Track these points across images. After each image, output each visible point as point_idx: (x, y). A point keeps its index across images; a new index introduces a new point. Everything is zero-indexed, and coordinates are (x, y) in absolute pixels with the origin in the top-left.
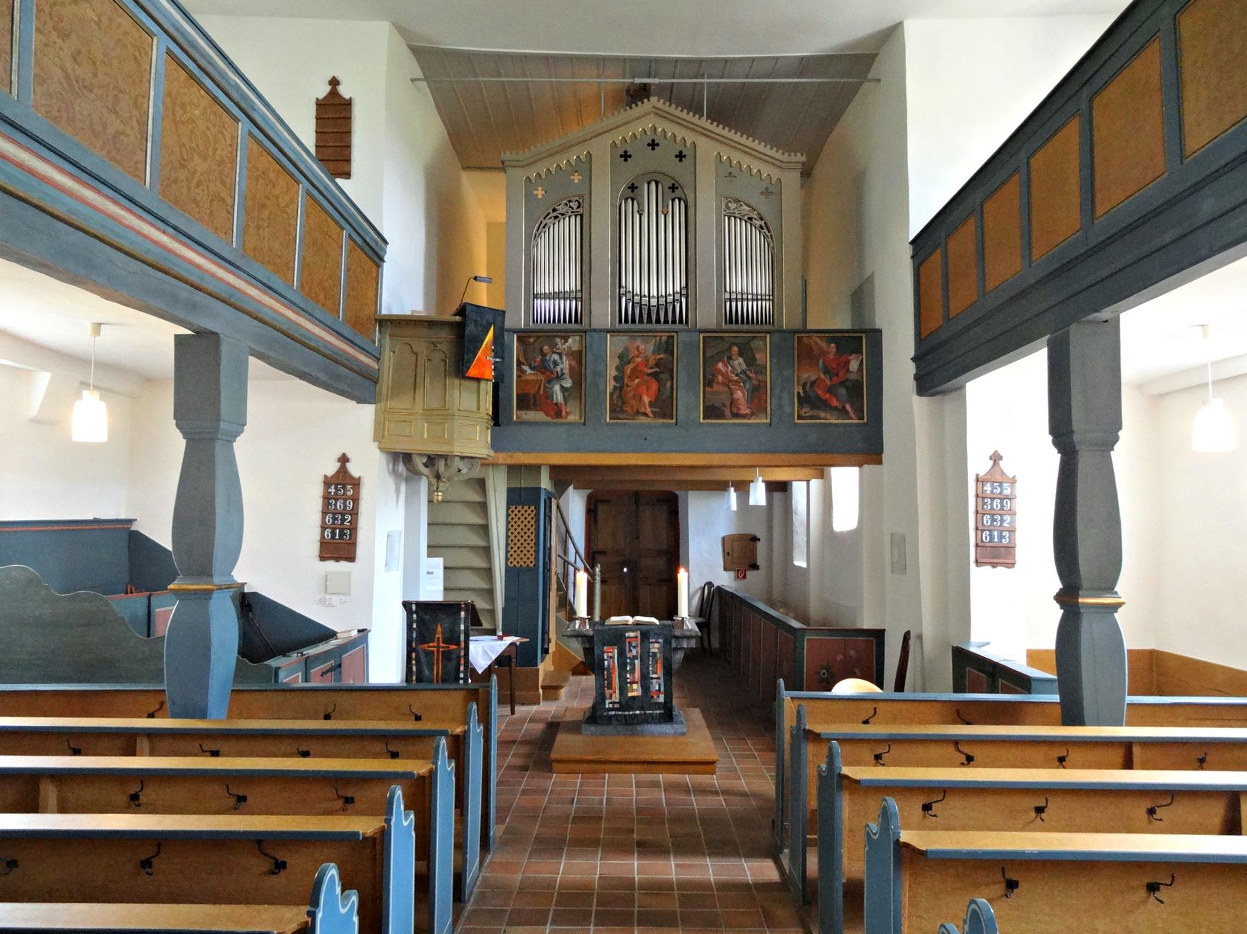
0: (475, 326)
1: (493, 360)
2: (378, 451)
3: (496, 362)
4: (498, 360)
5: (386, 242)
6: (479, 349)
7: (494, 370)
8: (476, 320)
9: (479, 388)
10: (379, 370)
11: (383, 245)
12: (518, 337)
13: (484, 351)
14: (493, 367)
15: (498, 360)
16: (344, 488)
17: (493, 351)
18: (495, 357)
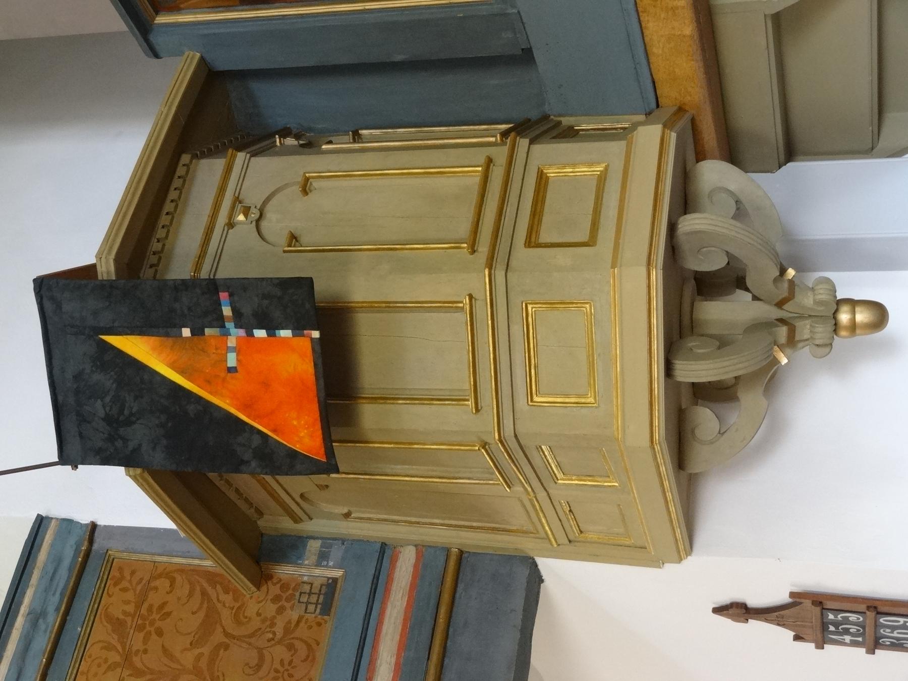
0: (129, 423)
1: (236, 334)
2: (691, 562)
3: (239, 319)
4: (227, 311)
5: (41, 523)
6: (208, 405)
7: (271, 334)
8: (108, 419)
9: (372, 307)
10: (416, 546)
11: (49, 537)
12: (157, 12)
13: (207, 382)
14: (260, 333)
15: (227, 311)
16: (836, 624)
17: (197, 332)
18: (220, 322)
